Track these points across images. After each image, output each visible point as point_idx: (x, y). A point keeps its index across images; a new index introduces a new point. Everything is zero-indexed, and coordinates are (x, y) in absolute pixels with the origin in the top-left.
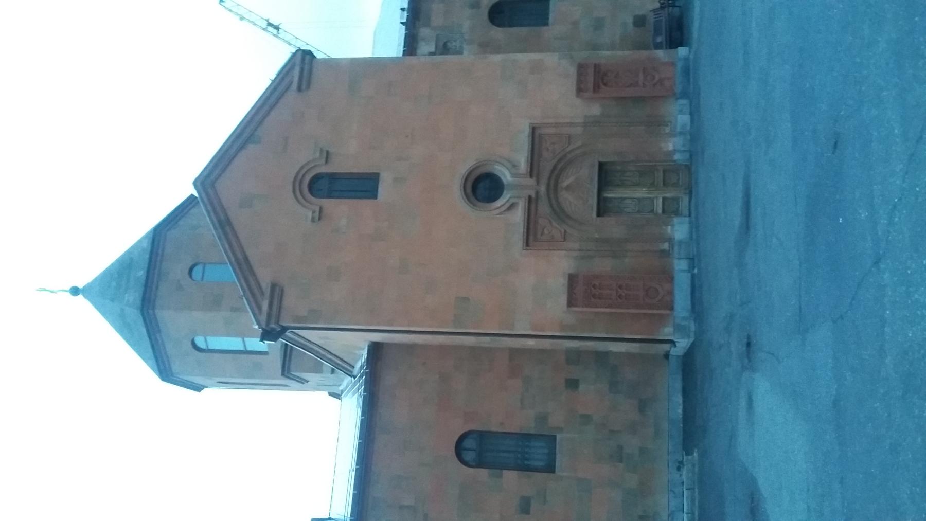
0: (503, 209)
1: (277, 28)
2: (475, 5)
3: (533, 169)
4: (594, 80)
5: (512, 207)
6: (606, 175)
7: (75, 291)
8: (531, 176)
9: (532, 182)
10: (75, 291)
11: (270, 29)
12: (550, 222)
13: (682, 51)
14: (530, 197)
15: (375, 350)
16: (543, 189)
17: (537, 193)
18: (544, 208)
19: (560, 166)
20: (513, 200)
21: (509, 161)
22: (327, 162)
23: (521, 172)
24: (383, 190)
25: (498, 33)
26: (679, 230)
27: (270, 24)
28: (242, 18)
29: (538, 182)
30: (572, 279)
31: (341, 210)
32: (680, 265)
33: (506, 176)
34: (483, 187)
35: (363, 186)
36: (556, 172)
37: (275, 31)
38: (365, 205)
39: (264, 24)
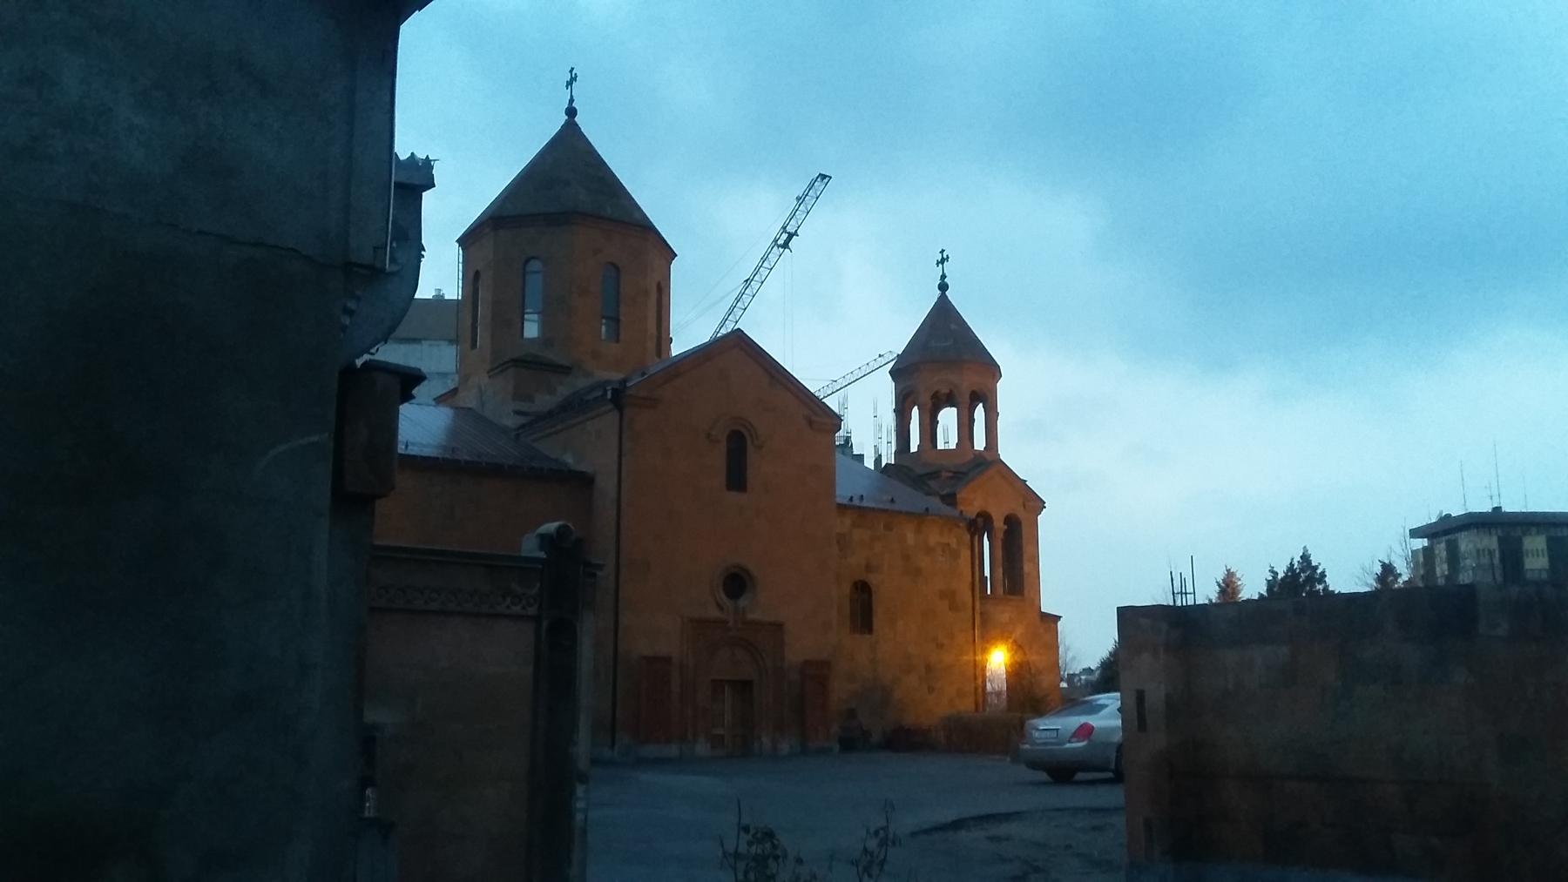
1: (786, 245)
2: (869, 568)
4: (817, 673)
5: (720, 607)
6: (744, 687)
7: (571, 112)
10: (571, 112)
11: (785, 236)
13: (837, 747)
15: (585, 481)
24: (734, 497)
25: (847, 589)
26: (702, 748)
27: (791, 236)
28: (798, 199)
30: (667, 660)
31: (718, 458)
32: (673, 750)
33: (743, 602)
34: (737, 583)
35: (737, 478)
37: (781, 242)
38: (721, 479)
39: (789, 229)
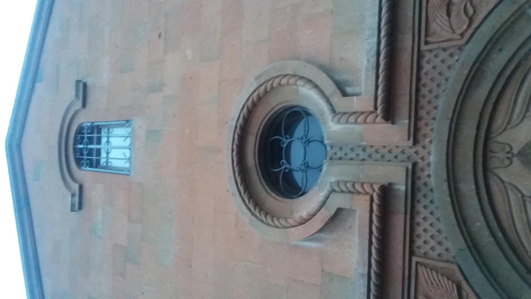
0: (317, 223)
3: (396, 91)
8: (389, 114)
9: (396, 134)
12: (459, 289)
14: (386, 192)
16: (433, 156)
17: (413, 174)
18: (436, 231)
19: (498, 61)
20: (339, 201)
21: (328, 71)
22: (84, 105)
23: (356, 104)
29: (415, 135)
36: (481, 93)
